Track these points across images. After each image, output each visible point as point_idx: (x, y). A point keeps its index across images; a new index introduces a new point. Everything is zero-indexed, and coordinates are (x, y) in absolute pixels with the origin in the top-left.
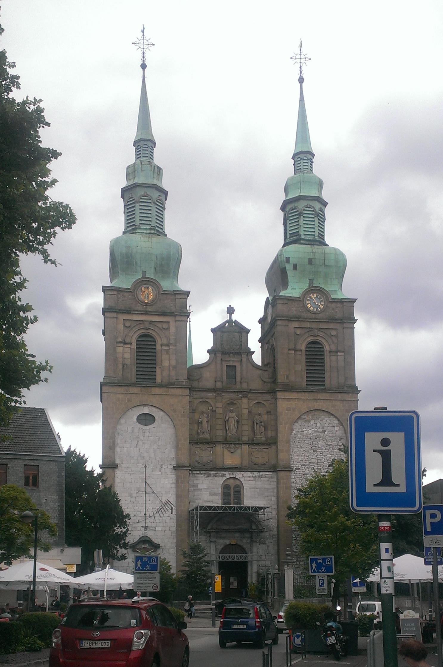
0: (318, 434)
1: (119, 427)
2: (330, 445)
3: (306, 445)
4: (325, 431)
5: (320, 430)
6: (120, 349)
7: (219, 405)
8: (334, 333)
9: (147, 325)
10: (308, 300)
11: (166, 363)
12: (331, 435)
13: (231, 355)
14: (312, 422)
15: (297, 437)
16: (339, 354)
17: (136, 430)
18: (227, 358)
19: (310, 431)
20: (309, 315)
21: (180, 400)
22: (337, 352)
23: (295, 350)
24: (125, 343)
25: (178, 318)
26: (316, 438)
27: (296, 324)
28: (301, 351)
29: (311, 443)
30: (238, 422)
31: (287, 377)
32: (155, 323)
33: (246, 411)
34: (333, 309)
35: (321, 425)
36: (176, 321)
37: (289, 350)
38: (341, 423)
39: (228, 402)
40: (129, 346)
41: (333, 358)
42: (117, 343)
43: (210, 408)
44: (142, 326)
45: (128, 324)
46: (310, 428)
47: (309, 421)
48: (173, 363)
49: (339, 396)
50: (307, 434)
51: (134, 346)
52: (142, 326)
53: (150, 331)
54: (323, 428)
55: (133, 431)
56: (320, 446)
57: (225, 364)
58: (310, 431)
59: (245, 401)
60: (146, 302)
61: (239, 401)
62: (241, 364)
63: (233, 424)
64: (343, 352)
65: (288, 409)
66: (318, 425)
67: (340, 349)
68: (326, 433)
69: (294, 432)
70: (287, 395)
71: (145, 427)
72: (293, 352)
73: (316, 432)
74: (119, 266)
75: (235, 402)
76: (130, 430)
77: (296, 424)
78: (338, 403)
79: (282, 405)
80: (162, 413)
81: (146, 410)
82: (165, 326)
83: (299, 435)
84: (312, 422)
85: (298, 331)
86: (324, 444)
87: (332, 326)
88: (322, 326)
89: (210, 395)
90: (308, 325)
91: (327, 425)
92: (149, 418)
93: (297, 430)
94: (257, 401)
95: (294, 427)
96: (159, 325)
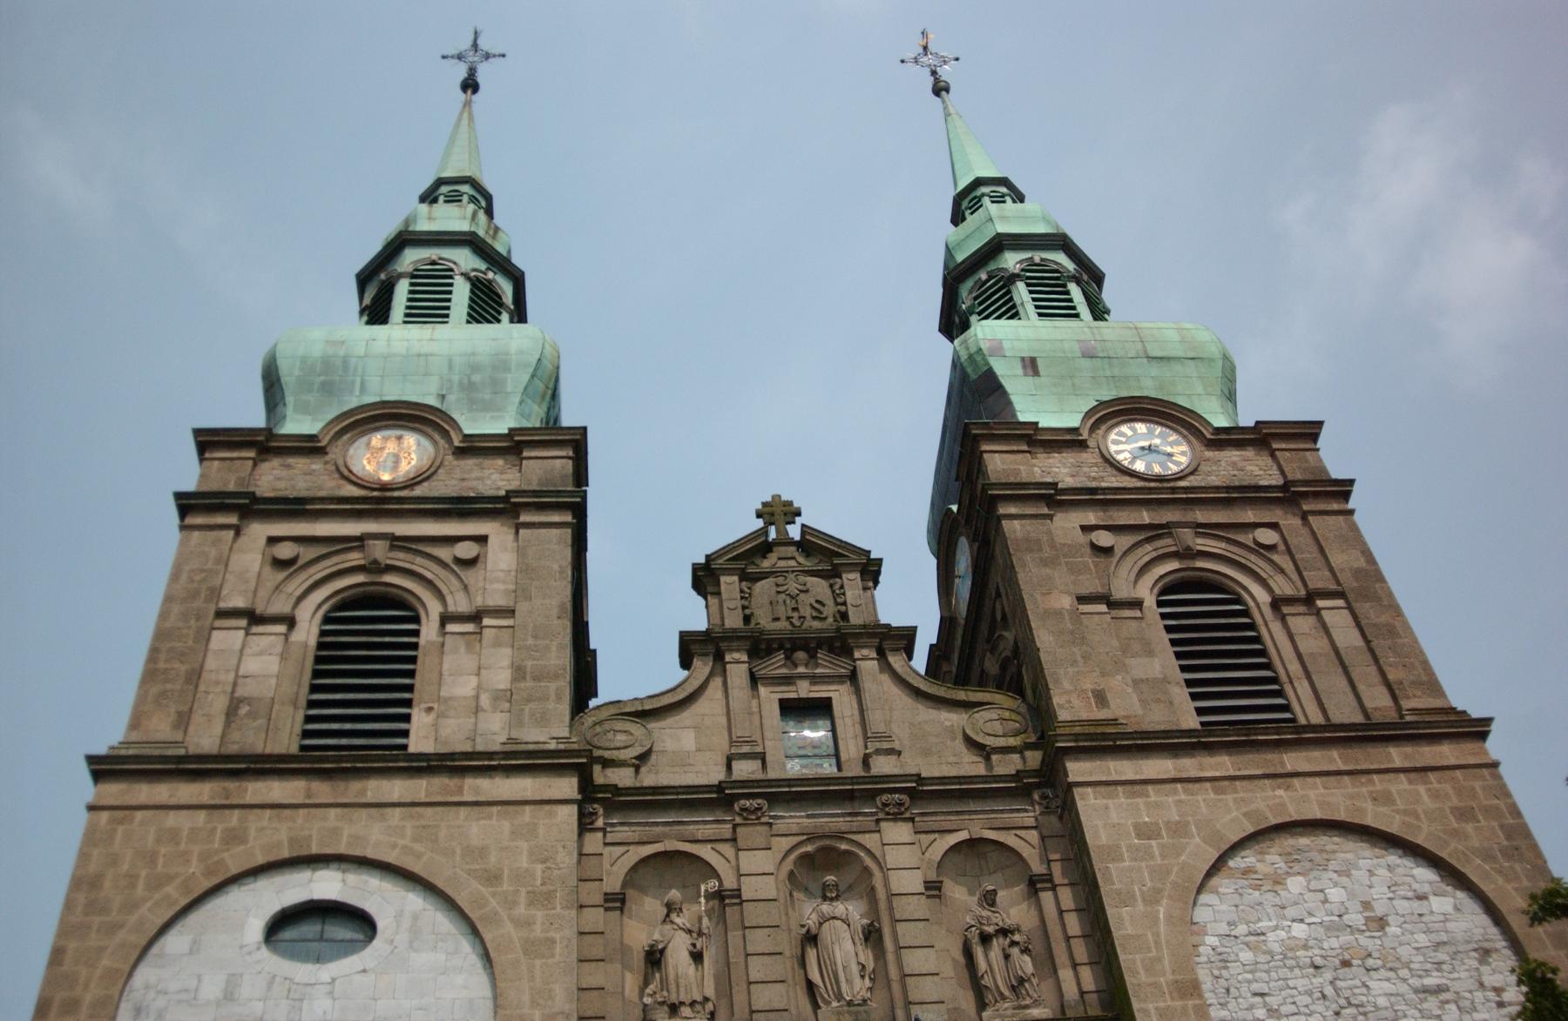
0: (1346, 938)
1: (144, 975)
2: (1439, 990)
3: (1306, 1000)
4: (1381, 923)
5: (1356, 918)
6: (228, 639)
7: (753, 861)
8: (1267, 537)
9: (379, 551)
10: (1116, 442)
11: (463, 687)
12: (1422, 939)
13: (801, 655)
14: (1295, 884)
15: (1235, 968)
16: (1320, 603)
17: (249, 988)
18: (776, 665)
19: (1299, 931)
20: (1140, 484)
21: (527, 838)
22: (1309, 599)
23: (1113, 604)
24: (254, 618)
25: (525, 518)
26: (1346, 964)
27: (1091, 517)
28: (1137, 604)
29: (1329, 991)
30: (872, 936)
31: (1101, 698)
32: (421, 547)
33: (911, 882)
34: (1234, 464)
35: (1351, 895)
36: (518, 527)
37: (1082, 599)
38: (1455, 877)
39: (809, 848)
40: (282, 628)
41: (1302, 624)
42: (222, 614)
43: (712, 885)
44: (355, 558)
45: (285, 551)
46: (1291, 912)
47: (1278, 881)
48: (501, 678)
49: (1397, 755)
50: (1290, 948)
51: (308, 632)
52: (355, 558)
53: (389, 578)
54: (1367, 905)
55: (229, 996)
56: (1382, 1001)
57: (770, 697)
58: (1299, 931)
59: (898, 832)
60: (386, 477)
61: (869, 840)
62: (858, 692)
63: (845, 949)
64: (1339, 595)
65: (1146, 832)
66: (1335, 894)
67: (1318, 579)
68: (1391, 930)
69: (1211, 940)
70: (1123, 768)
71: (303, 971)
72: (1103, 608)
73: (1330, 929)
74: (290, 399)
75: (844, 846)
76: (212, 988)
77: (1205, 898)
78: (1401, 784)
79: (1104, 816)
80: (415, 901)
81: (327, 885)
82: (466, 550)
83: (1246, 956)
84: (1295, 884)
85: (1104, 539)
86: (1403, 988)
87: (1249, 516)
88: (1201, 516)
89: (705, 825)
90: (1145, 517)
91: (1379, 893)
92: (340, 931)
93: (1223, 928)
94: (963, 836)
95: (1201, 914)
96: (444, 553)
